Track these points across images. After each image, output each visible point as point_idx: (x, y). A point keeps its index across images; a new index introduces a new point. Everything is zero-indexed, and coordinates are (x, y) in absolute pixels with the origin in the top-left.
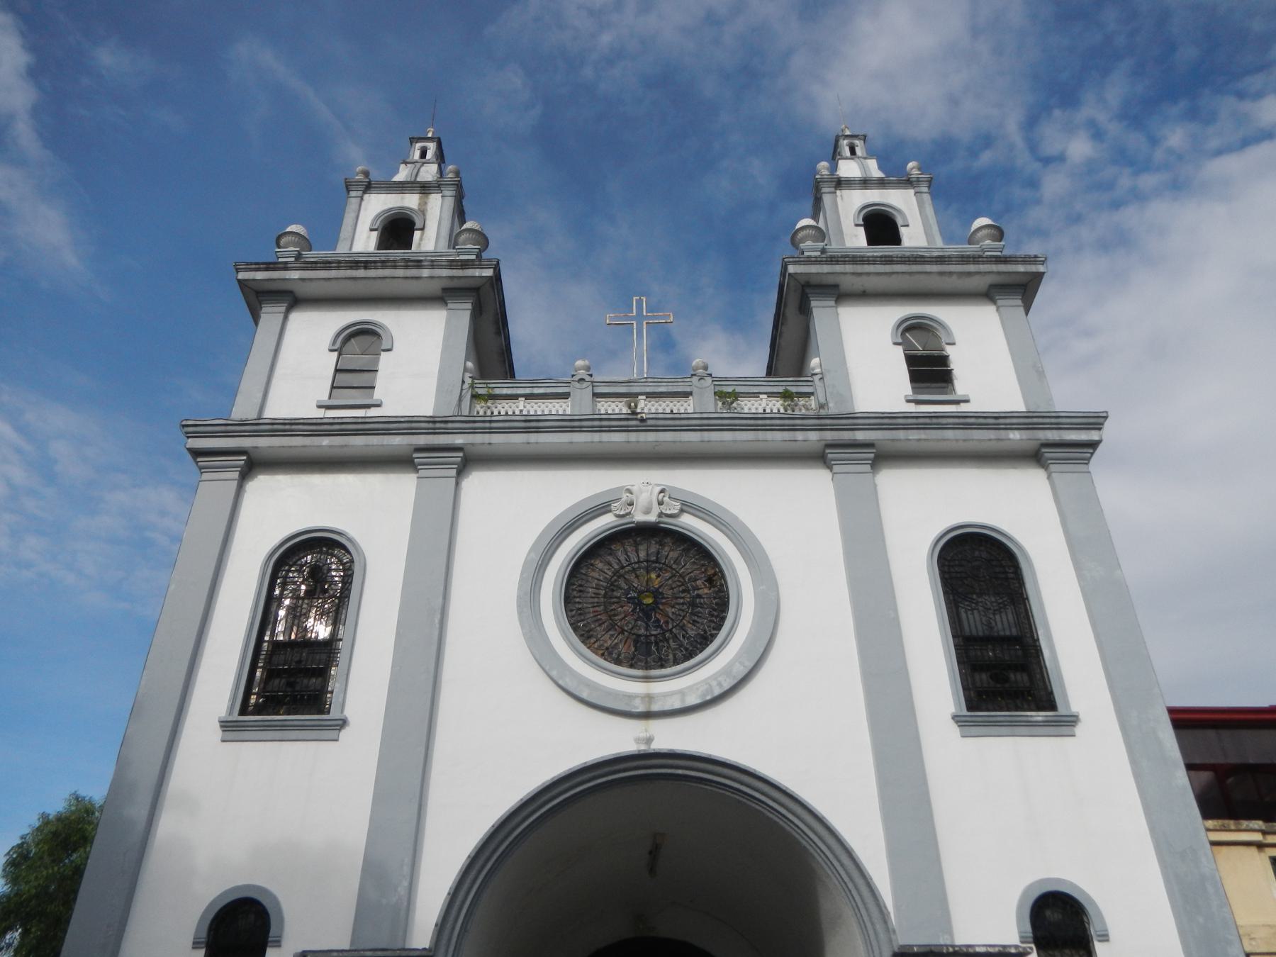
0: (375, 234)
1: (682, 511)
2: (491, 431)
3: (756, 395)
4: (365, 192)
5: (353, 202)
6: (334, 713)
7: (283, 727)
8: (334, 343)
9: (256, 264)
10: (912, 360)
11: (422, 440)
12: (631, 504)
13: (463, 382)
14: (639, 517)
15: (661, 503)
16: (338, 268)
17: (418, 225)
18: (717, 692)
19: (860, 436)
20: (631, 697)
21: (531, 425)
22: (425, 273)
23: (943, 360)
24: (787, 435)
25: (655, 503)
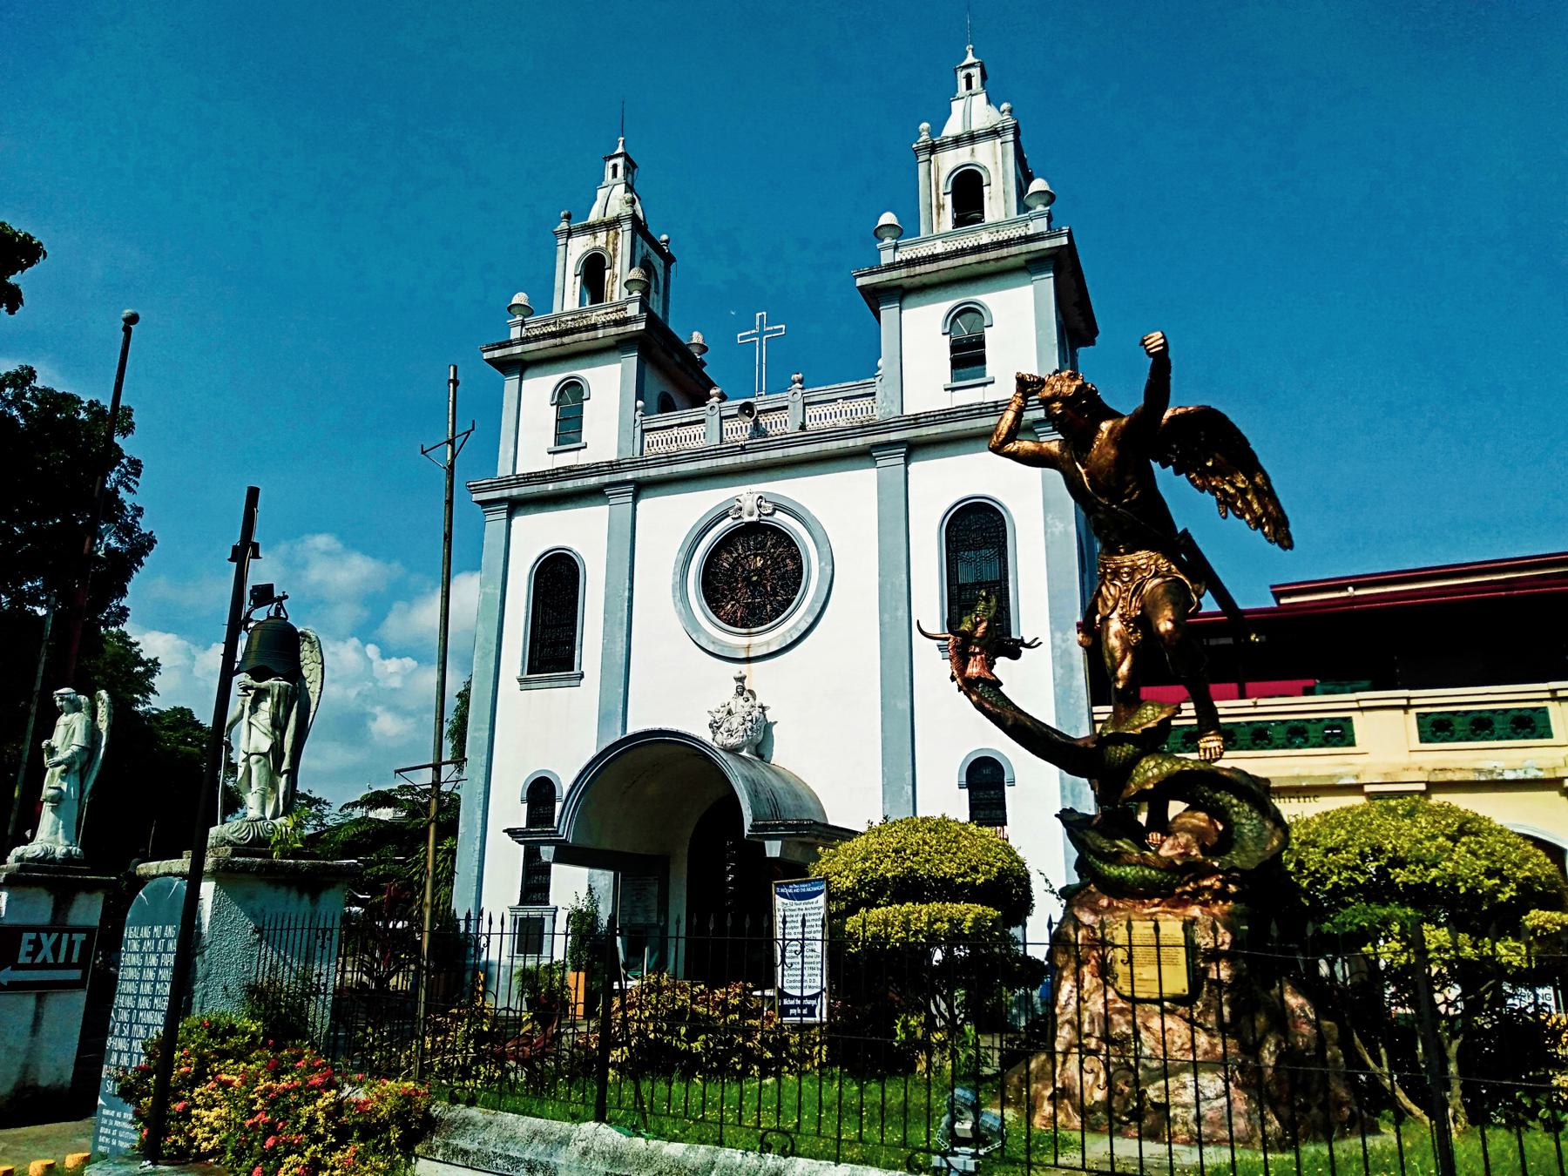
0: (579, 278)
1: (775, 510)
2: (648, 467)
3: (835, 400)
4: (568, 238)
5: (561, 249)
6: (576, 670)
7: (550, 680)
8: (553, 399)
9: (493, 345)
10: (955, 347)
11: (606, 479)
12: (741, 509)
13: (635, 421)
14: (747, 519)
15: (759, 506)
16: (544, 339)
17: (608, 264)
18: (789, 641)
19: (894, 436)
20: (736, 648)
21: (671, 459)
22: (600, 333)
23: (981, 343)
24: (842, 444)
25: (756, 507)
